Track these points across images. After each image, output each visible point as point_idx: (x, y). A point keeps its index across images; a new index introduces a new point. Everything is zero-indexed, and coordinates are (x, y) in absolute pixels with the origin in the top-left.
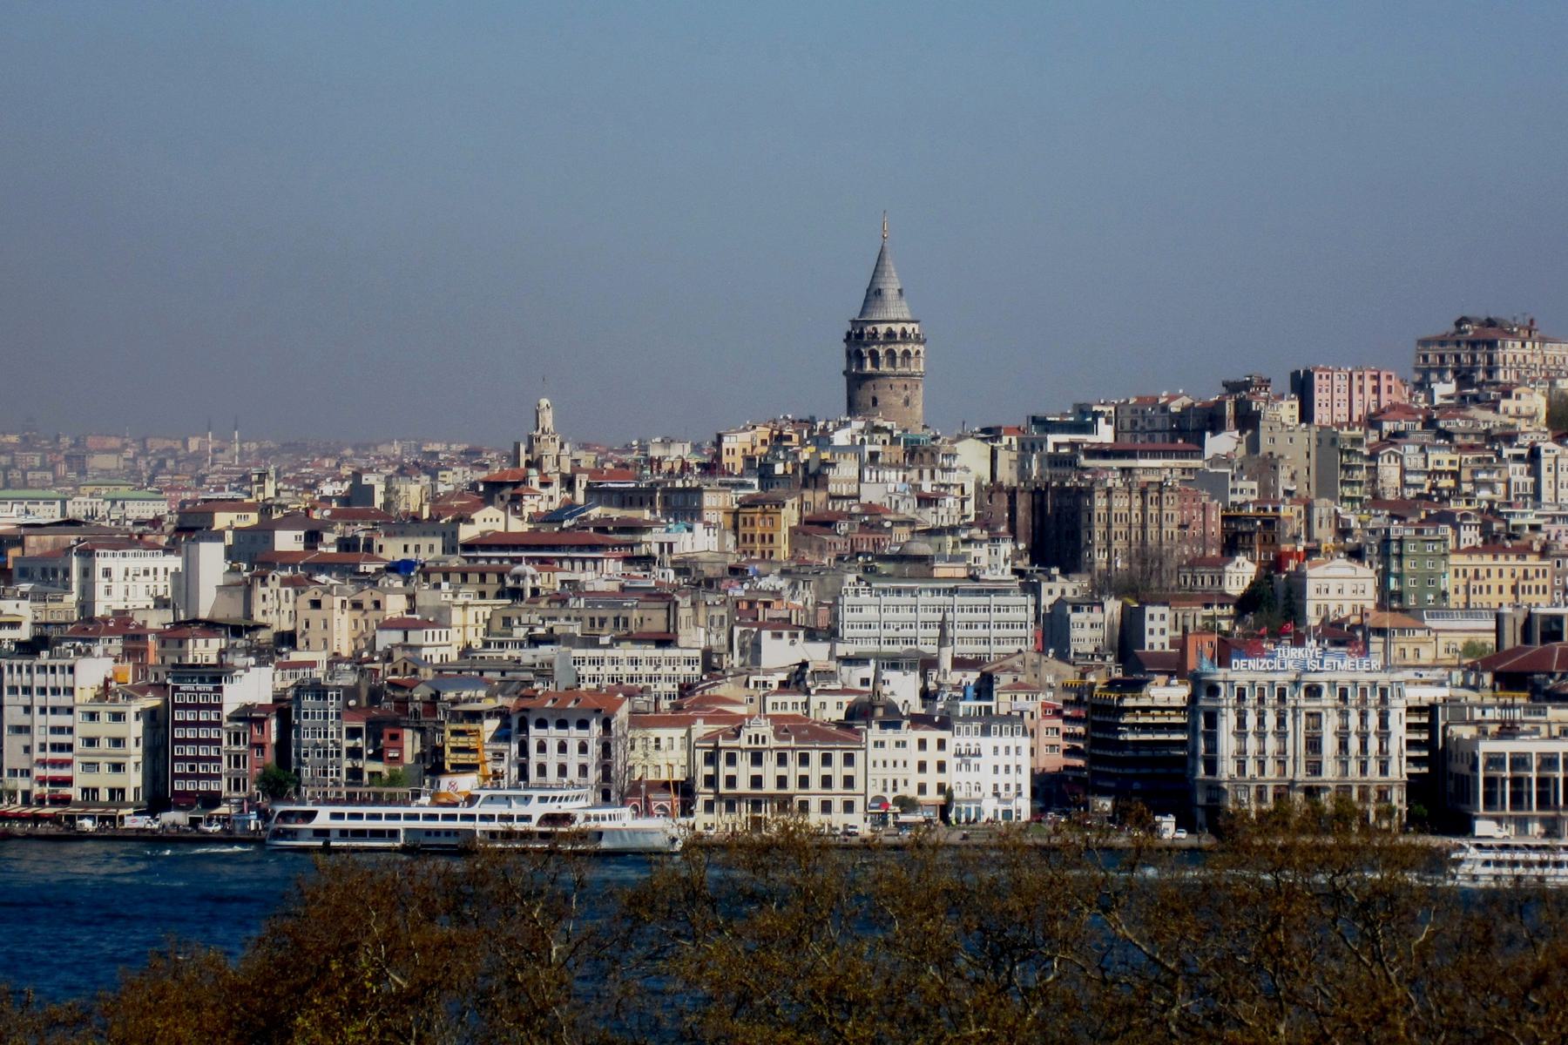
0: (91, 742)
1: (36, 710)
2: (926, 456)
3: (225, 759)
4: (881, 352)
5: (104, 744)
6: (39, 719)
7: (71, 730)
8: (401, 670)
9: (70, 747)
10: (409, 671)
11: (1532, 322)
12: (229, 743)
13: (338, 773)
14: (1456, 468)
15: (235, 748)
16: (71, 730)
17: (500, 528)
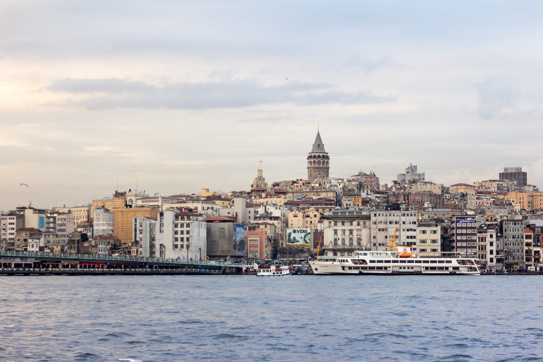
0: (423, 242)
1: (401, 230)
2: (365, 186)
3: (478, 247)
4: (322, 161)
5: (429, 242)
6: (403, 233)
7: (415, 237)
8: (490, 220)
9: (415, 244)
10: (493, 220)
11: (374, 173)
12: (479, 241)
13: (522, 252)
14: (449, 198)
15: (482, 243)
16: (415, 237)
17: (291, 200)
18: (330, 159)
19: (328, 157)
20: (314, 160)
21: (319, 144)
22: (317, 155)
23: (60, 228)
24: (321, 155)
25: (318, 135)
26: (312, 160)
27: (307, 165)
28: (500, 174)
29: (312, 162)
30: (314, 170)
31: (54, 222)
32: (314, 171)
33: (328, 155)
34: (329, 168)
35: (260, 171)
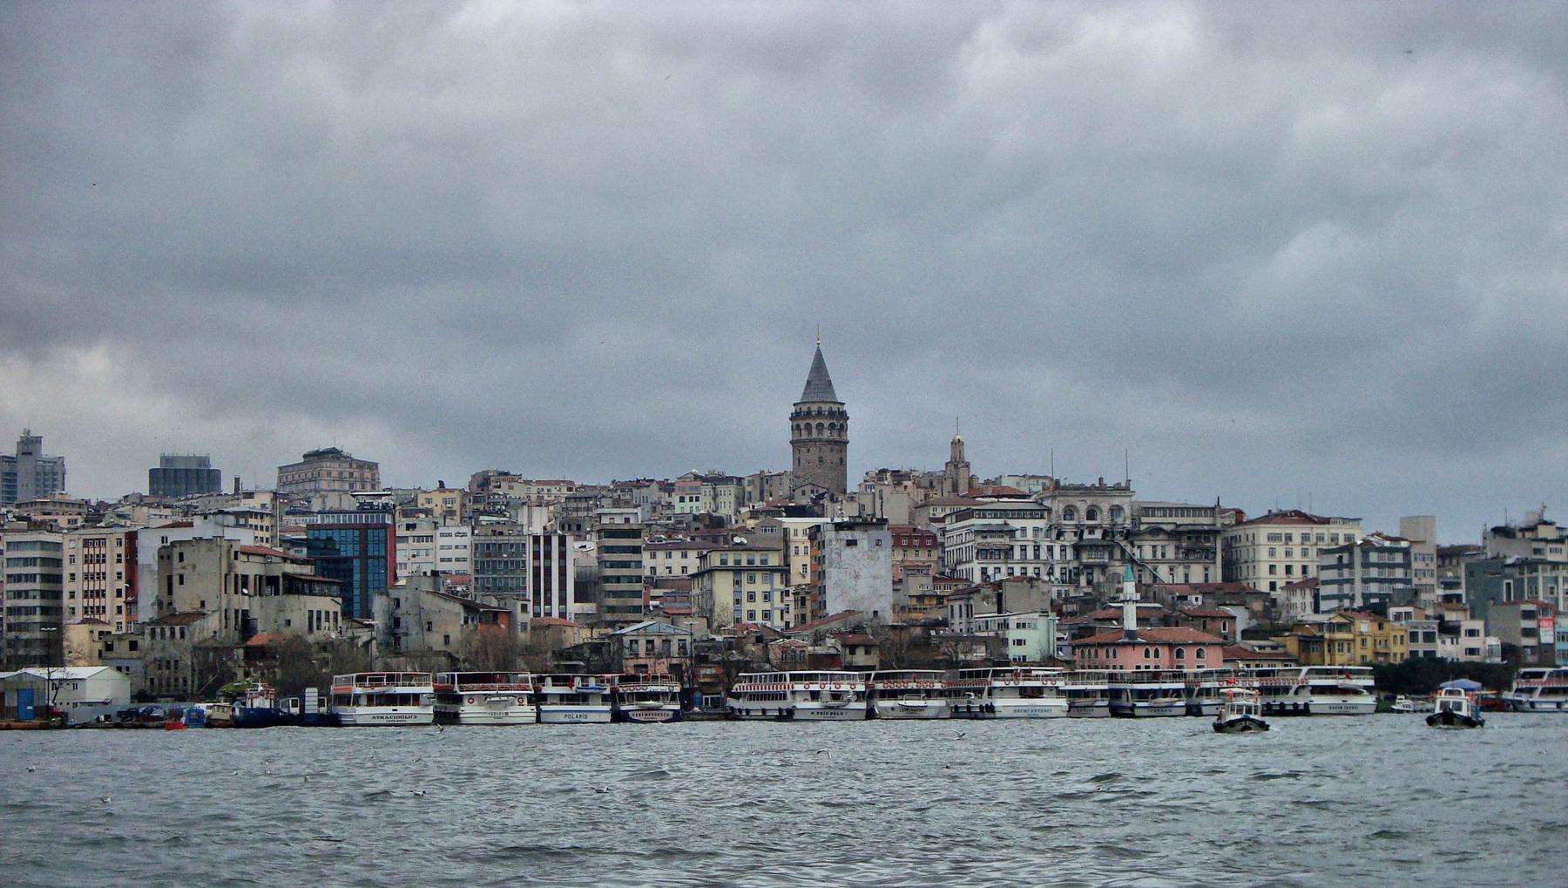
18: (848, 418)
19: (843, 416)
20: (832, 421)
21: (819, 377)
22: (815, 408)
23: (1420, 583)
24: (825, 408)
25: (819, 357)
26: (826, 423)
27: (788, 435)
28: (153, 472)
29: (826, 426)
30: (830, 447)
31: (1406, 565)
32: (832, 450)
33: (845, 408)
34: (848, 443)
35: (957, 444)
